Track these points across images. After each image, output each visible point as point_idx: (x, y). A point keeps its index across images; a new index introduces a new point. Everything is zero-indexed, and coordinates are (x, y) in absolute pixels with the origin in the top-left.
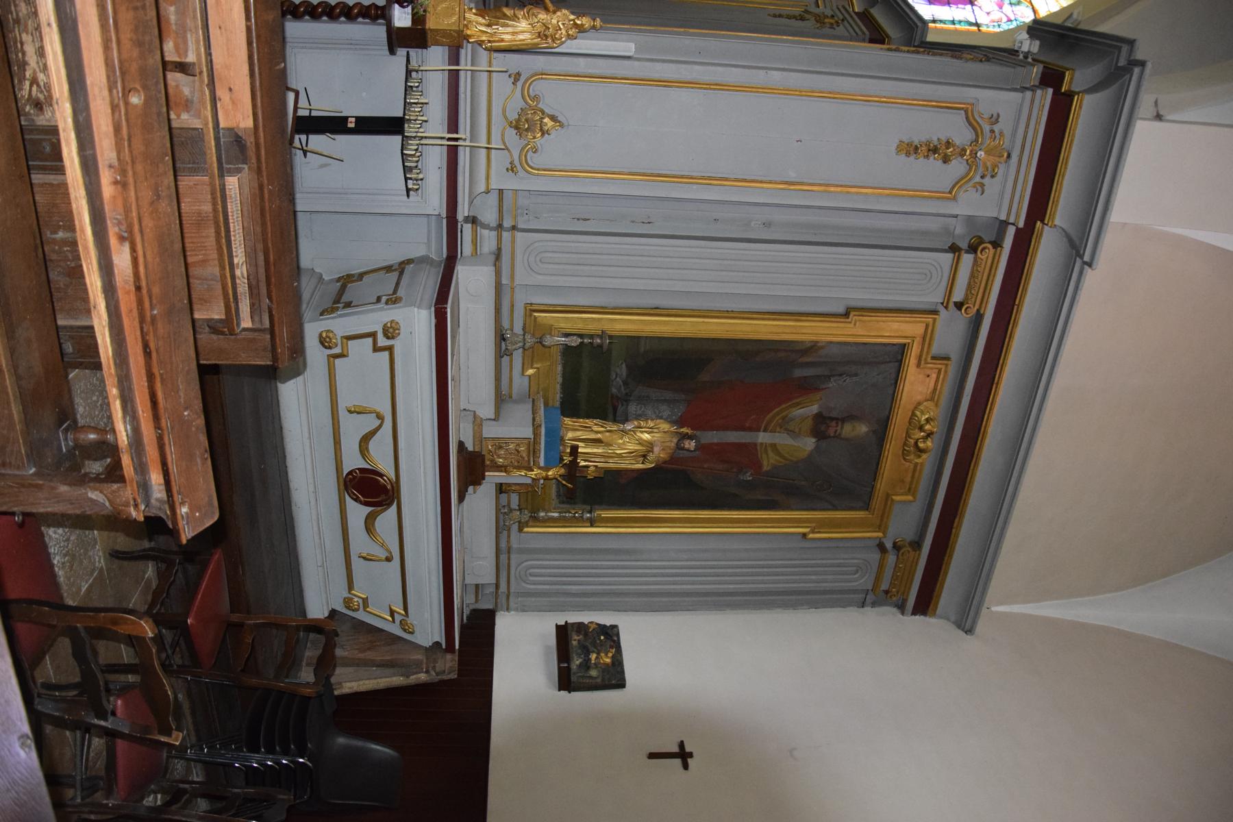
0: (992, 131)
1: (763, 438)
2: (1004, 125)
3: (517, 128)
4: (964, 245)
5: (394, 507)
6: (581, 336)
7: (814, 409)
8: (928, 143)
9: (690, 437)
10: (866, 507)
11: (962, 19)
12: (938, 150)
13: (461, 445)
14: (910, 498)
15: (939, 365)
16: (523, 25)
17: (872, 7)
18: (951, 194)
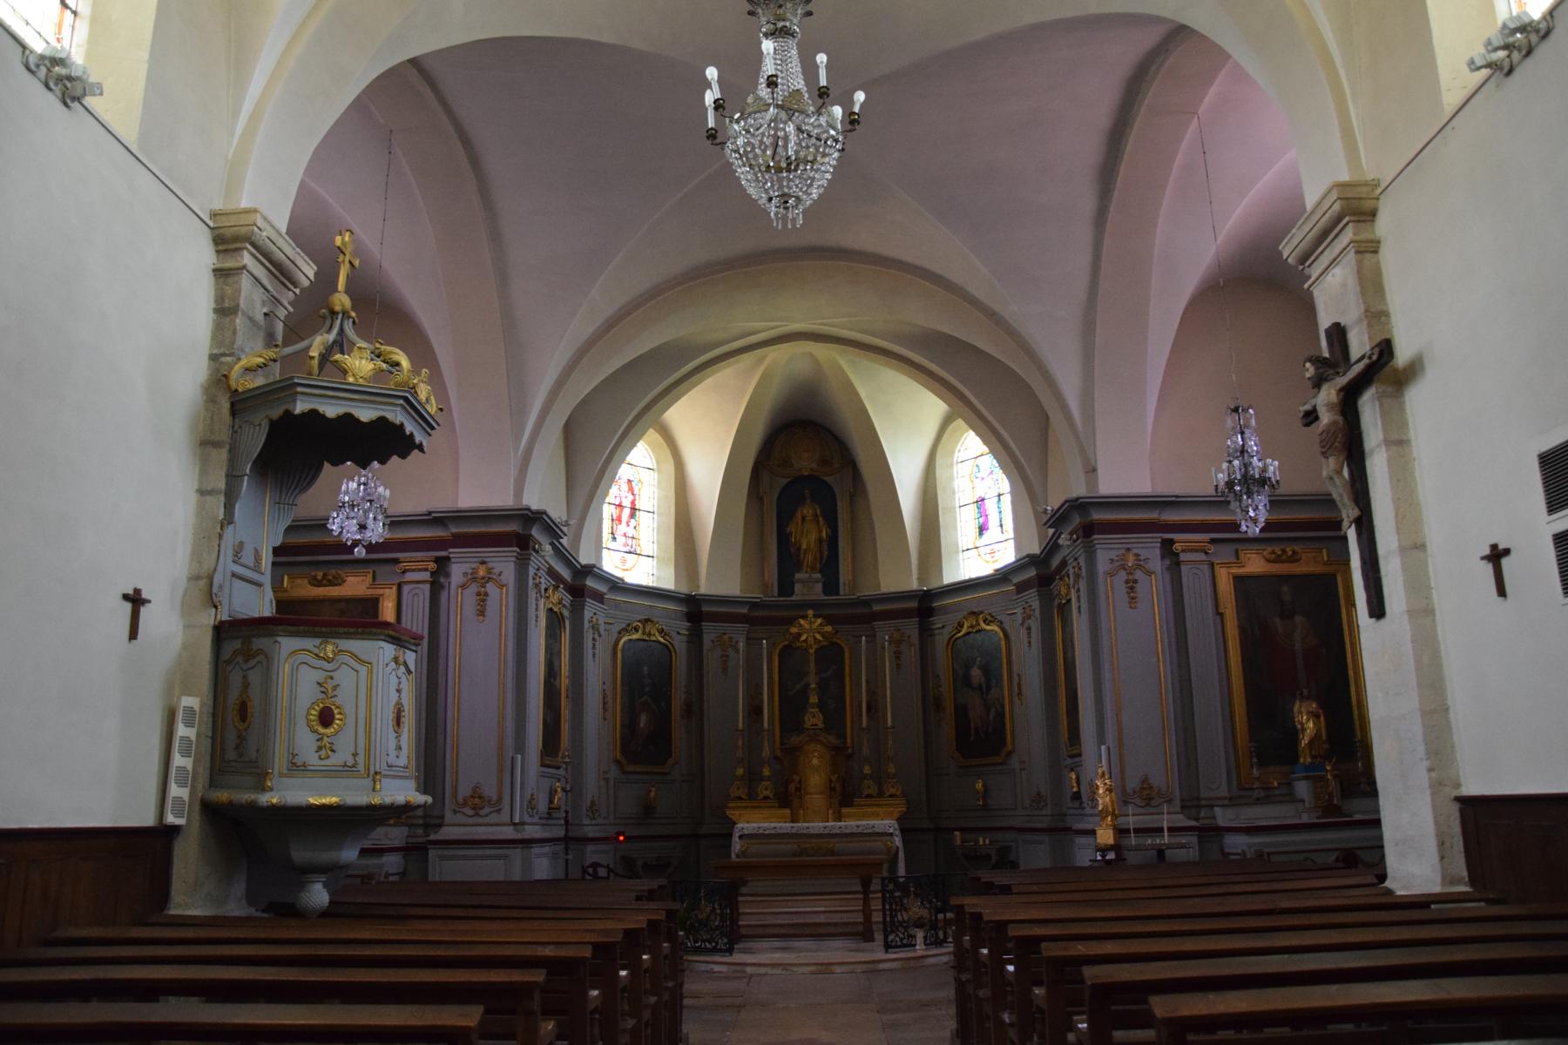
0: (1117, 561)
1: (1298, 647)
2: (1113, 554)
5: (1359, 852)
7: (1277, 620)
8: (1128, 593)
9: (1301, 693)
10: (1334, 576)
12: (1131, 586)
13: (1318, 818)
14: (1324, 551)
15: (1241, 554)
17: (1011, 581)
18: (1149, 573)
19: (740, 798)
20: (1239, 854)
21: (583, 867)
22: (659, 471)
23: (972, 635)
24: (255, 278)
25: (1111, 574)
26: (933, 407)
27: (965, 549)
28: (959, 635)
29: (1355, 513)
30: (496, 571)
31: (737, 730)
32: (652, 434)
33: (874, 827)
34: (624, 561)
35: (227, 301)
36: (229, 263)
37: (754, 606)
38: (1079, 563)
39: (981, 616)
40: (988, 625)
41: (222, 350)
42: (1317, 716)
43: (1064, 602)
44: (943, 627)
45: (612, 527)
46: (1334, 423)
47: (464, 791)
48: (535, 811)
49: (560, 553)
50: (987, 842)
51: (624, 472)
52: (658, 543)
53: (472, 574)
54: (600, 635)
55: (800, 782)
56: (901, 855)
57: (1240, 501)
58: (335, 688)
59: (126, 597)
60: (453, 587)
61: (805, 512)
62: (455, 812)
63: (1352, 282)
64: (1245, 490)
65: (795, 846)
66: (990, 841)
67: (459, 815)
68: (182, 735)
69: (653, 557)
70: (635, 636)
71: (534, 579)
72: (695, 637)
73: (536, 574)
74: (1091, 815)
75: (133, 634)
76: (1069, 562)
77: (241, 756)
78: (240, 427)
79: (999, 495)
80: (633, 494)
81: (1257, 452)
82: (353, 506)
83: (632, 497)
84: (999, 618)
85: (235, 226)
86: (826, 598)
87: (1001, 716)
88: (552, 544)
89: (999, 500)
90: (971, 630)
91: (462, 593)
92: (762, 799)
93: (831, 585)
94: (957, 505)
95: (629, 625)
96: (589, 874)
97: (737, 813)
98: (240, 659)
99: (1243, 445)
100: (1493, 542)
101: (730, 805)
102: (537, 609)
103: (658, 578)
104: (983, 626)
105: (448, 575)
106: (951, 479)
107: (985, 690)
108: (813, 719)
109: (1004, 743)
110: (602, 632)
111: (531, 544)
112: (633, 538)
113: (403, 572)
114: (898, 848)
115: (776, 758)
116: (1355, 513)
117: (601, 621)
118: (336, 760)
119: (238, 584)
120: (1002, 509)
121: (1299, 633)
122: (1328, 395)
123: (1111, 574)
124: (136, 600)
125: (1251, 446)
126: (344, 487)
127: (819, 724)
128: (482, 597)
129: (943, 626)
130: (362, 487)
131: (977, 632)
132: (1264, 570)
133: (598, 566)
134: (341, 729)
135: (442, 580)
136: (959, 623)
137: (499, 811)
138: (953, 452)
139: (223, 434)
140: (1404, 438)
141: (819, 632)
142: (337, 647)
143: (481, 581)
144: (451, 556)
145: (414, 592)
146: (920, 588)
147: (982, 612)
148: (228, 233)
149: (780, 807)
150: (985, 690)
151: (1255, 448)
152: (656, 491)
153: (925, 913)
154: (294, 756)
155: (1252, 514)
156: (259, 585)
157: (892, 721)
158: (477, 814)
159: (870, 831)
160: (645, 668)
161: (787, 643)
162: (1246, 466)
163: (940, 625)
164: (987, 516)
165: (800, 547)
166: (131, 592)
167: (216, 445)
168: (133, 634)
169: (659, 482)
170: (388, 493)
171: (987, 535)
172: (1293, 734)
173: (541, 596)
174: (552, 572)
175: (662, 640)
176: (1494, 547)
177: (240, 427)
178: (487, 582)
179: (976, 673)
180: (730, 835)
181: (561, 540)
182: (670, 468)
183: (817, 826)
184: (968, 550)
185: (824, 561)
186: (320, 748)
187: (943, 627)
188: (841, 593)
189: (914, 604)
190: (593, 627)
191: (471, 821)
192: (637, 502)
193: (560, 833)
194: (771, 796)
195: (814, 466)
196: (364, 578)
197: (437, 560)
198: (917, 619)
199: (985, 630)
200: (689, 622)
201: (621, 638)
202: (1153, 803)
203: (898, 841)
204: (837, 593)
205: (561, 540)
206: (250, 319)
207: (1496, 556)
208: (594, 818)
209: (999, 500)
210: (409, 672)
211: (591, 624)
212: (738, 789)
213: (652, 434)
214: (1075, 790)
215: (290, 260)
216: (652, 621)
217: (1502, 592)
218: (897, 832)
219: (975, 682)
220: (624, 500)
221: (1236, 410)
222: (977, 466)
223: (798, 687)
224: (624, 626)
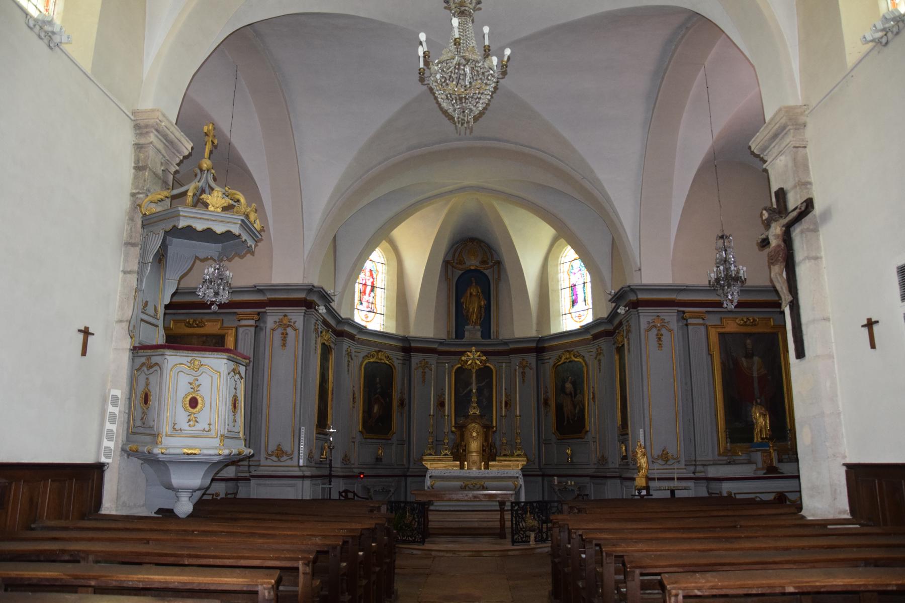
0: (652, 322)
1: (755, 374)
2: (650, 319)
3: (667, 461)
4: (685, 322)
5: (786, 494)
6: (727, 438)
7: (743, 359)
8: (658, 341)
9: (756, 402)
10: (776, 334)
11: (582, 289)
12: (659, 338)
13: (764, 474)
14: (772, 319)
16: (642, 461)
17: (590, 333)
18: (670, 330)
19: (431, 455)
20: (718, 494)
21: (339, 492)
22: (388, 265)
23: (567, 363)
24: (158, 150)
25: (648, 330)
26: (547, 232)
27: (563, 314)
28: (559, 363)
29: (790, 298)
30: (293, 321)
31: (430, 415)
32: (384, 244)
33: (507, 473)
34: (367, 317)
35: (141, 162)
36: (142, 141)
37: (441, 343)
38: (629, 324)
39: (572, 353)
40: (576, 358)
41: (137, 191)
42: (764, 415)
43: (620, 345)
44: (550, 358)
45: (360, 297)
46: (779, 246)
47: (272, 447)
48: (313, 459)
49: (331, 312)
50: (573, 483)
51: (368, 265)
52: (387, 307)
53: (279, 322)
54: (352, 359)
55: (465, 446)
56: (523, 487)
57: (723, 290)
58: (199, 386)
59: (80, 331)
60: (268, 330)
61: (472, 291)
62: (267, 459)
63: (790, 164)
64: (726, 284)
65: (462, 483)
66: (574, 483)
67: (268, 460)
68: (111, 411)
69: (383, 314)
70: (371, 360)
71: (315, 326)
72: (407, 361)
73: (316, 323)
74: (634, 469)
75: (84, 353)
76: (623, 323)
77: (144, 423)
78: (147, 235)
79: (584, 283)
80: (373, 278)
81: (734, 262)
82: (211, 282)
83: (372, 280)
84: (582, 354)
85: (146, 119)
86: (483, 340)
87: (582, 411)
88: (325, 306)
89: (584, 286)
90: (566, 361)
91: (273, 333)
92: (443, 455)
93: (486, 334)
94: (560, 289)
95: (369, 353)
96: (342, 496)
97: (429, 463)
98: (145, 369)
99: (726, 257)
100: (869, 317)
101: (425, 458)
102: (316, 343)
103: (386, 327)
104: (574, 358)
105: (265, 322)
106: (557, 273)
107: (573, 395)
108: (474, 411)
109: (584, 426)
110: (353, 357)
111: (313, 305)
112: (372, 303)
113: (239, 321)
114: (521, 485)
115: (452, 432)
116: (790, 298)
117: (353, 351)
118: (199, 427)
119: (142, 324)
120: (586, 291)
121: (756, 367)
122: (776, 230)
123: (648, 330)
124: (86, 332)
125: (731, 258)
126: (206, 271)
127: (477, 413)
128: (285, 335)
129: (551, 358)
130: (217, 271)
131: (569, 362)
132: (737, 330)
133: (352, 319)
134: (202, 409)
135: (262, 325)
136: (559, 356)
137: (292, 458)
138: (558, 258)
139: (138, 239)
140: (819, 255)
141: (478, 360)
142: (200, 363)
143: (284, 325)
144: (267, 311)
145: (247, 331)
146: (538, 336)
147: (572, 351)
148: (142, 123)
149: (454, 460)
150: (573, 395)
151: (733, 259)
152: (386, 276)
153: (535, 523)
154: (175, 424)
155: (730, 297)
156: (157, 326)
157: (520, 412)
158: (279, 460)
159: (505, 475)
160: (378, 379)
161: (460, 365)
162: (727, 269)
163: (548, 357)
164: (577, 295)
165: (469, 310)
166: (83, 329)
167: (134, 245)
168: (84, 353)
169: (388, 271)
170: (231, 275)
171: (577, 307)
172: (750, 426)
173: (319, 336)
174: (325, 322)
175: (387, 362)
176: (869, 320)
177: (147, 235)
178: (288, 327)
179: (568, 386)
180: (425, 476)
181: (331, 304)
182: (394, 263)
183: (475, 471)
184: (565, 314)
185: (482, 319)
186: (189, 421)
187: (550, 358)
188: (492, 337)
189: (534, 345)
190: (348, 354)
191: (275, 464)
192: (375, 283)
193: (327, 472)
194: (449, 453)
195: (478, 264)
196: (217, 323)
197: (258, 314)
198: (535, 354)
199: (574, 361)
200: (403, 352)
201: (364, 361)
202: (669, 463)
203: (521, 482)
204: (489, 338)
205: (331, 304)
206: (154, 173)
207: (870, 324)
208: (347, 464)
209: (584, 286)
210: (242, 378)
211: (347, 352)
212: (430, 449)
213: (384, 244)
214: (624, 454)
215: (178, 139)
216: (382, 352)
217: (873, 346)
218: (521, 476)
219: (568, 391)
220: (367, 281)
221: (722, 237)
222: (572, 266)
223: (465, 392)
224: (366, 354)
